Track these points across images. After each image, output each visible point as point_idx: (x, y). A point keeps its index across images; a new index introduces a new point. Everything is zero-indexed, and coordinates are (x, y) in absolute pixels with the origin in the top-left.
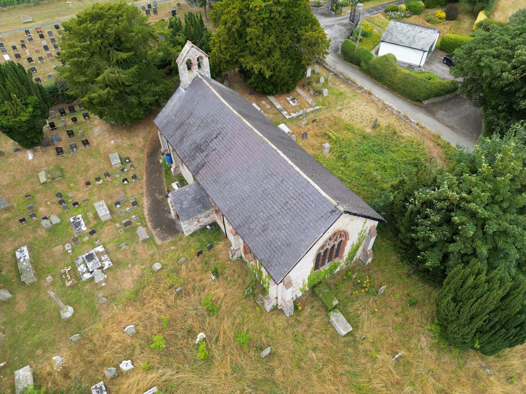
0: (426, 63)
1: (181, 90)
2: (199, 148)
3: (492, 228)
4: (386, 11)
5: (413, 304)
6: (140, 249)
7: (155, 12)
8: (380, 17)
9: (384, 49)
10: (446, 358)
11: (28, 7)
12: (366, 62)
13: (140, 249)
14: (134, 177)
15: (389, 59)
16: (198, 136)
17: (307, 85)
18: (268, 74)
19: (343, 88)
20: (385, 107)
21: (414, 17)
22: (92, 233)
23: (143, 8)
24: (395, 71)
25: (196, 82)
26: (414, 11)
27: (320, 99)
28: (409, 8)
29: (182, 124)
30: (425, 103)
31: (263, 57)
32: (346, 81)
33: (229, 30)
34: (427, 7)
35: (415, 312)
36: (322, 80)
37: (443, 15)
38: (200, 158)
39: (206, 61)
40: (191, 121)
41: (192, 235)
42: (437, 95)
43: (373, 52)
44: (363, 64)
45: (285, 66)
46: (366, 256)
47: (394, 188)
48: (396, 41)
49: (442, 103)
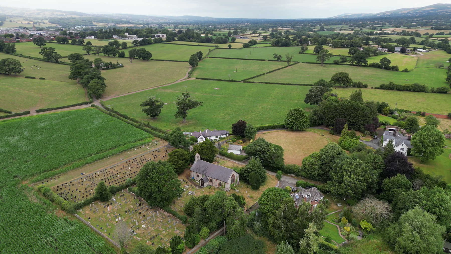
0: (241, 153)
1: (195, 162)
2: (204, 171)
3: (253, 169)
4: (227, 142)
5: (248, 187)
6: (198, 190)
7: (160, 151)
8: (225, 144)
9: (230, 151)
10: (254, 191)
11: (116, 156)
12: (227, 155)
13: (198, 190)
14: (188, 182)
15: (231, 153)
16: (203, 169)
17: (215, 161)
18: (208, 159)
19: (223, 161)
20: (234, 163)
21: (234, 143)
22: (187, 190)
23: (155, 151)
24: (234, 155)
25: (198, 160)
26: (234, 142)
27: (219, 163)
28: (232, 141)
29: (198, 168)
30: (243, 161)
31: (206, 155)
32: (223, 159)
33: (199, 151)
34: (237, 140)
35: (248, 189)
36: (218, 160)
37: (242, 141)
38: (205, 172)
39: (200, 156)
40: (200, 167)
41: (207, 186)
42: (245, 159)
43: (227, 152)
44: (226, 155)
45: (211, 156)
46: (238, 183)
47: (240, 171)
48: (231, 149)
49: (246, 161)
